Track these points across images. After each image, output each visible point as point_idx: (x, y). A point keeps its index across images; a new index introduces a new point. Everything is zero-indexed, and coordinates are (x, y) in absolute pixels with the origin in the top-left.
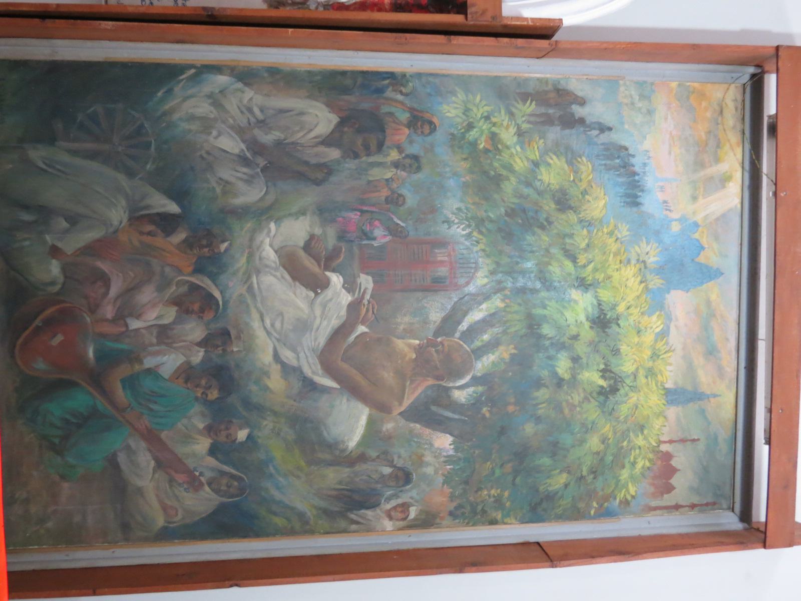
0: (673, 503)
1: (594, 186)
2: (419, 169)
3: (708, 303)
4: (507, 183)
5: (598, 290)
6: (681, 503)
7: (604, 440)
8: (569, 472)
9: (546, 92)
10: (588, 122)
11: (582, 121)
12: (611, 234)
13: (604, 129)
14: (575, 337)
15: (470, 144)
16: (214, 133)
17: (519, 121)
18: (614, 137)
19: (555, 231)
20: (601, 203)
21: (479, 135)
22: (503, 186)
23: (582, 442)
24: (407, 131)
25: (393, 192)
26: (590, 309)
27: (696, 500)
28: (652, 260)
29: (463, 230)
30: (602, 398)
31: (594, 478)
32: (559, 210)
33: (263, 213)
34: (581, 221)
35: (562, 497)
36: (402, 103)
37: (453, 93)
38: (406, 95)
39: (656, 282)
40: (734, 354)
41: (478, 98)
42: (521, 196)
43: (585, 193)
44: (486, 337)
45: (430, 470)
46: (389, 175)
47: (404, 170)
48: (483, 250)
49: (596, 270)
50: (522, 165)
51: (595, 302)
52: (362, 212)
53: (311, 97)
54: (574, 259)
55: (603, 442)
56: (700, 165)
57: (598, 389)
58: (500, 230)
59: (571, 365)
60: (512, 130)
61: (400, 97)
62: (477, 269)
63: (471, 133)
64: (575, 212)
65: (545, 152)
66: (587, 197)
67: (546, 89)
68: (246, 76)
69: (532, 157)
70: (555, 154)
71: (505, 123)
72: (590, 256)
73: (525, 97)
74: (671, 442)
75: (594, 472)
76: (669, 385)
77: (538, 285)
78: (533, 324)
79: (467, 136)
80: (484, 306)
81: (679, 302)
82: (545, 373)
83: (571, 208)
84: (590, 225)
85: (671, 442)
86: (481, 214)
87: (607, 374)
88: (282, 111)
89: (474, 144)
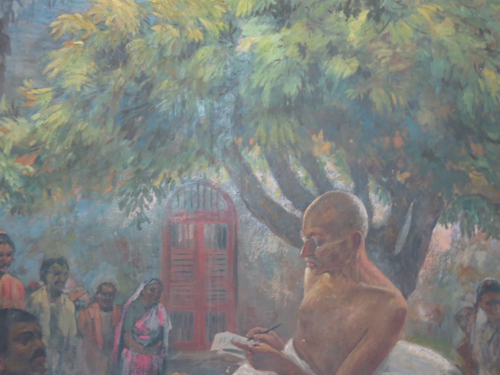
1: (91, 13)
2: (62, 261)
4: (85, 136)
5: (238, 14)
8: (482, 66)
14: (302, 49)
15: (27, 185)
19: (155, 69)
22: (89, 142)
23: (441, 46)
25: (95, 300)
26: (264, 27)
29: (151, 200)
30: (384, 17)
31: (489, 32)
32: (125, 63)
34: (142, 33)
42: (104, 117)
43: (101, 26)
44: (301, 173)
45: (481, 257)
46: (70, 306)
48: (180, 173)
49: (210, 17)
50: (60, 113)
51: (254, 19)
52: (123, 345)
54: (195, 46)
55: (442, 18)
57: (372, 22)
58: (151, 148)
59: (340, 56)
62: (207, 183)
63: (12, 183)
64: (128, 41)
66: (107, 23)
69: (49, 97)
70: (45, 65)
72: (191, 22)
75: (481, 33)
77: (229, 97)
78: (284, 107)
79: (15, 189)
80: (258, 175)
82: (351, 93)
84: (146, 21)
86: (125, 175)
87: (352, 7)
89: (28, 180)
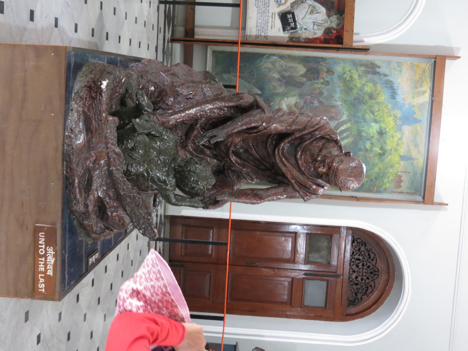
0: (401, 191)
2: (328, 85)
3: (416, 130)
4: (354, 90)
6: (404, 191)
7: (380, 169)
8: (368, 178)
9: (368, 64)
10: (380, 73)
11: (379, 73)
12: (386, 107)
13: (385, 75)
14: (372, 137)
15: (344, 78)
16: (272, 72)
17: (359, 72)
18: (388, 78)
19: (368, 105)
20: (383, 97)
21: (347, 76)
24: (326, 74)
25: (320, 91)
26: (377, 129)
27: (409, 191)
28: (399, 115)
30: (380, 156)
31: (376, 180)
33: (284, 95)
34: (376, 103)
35: (365, 185)
36: (325, 66)
37: (340, 64)
38: (326, 64)
39: (399, 122)
40: (424, 147)
41: (347, 65)
42: (358, 94)
43: (378, 94)
44: (345, 135)
46: (320, 86)
47: (324, 85)
49: (380, 117)
51: (379, 127)
52: (311, 96)
53: (299, 63)
54: (373, 114)
55: (379, 170)
56: (416, 87)
57: (379, 153)
59: (371, 145)
60: (357, 75)
61: (324, 64)
62: (343, 114)
64: (375, 100)
65: (367, 82)
67: (368, 63)
68: (282, 57)
71: (355, 73)
72: (379, 113)
73: (361, 65)
74: (401, 172)
75: (376, 178)
76: (402, 154)
77: (362, 121)
78: (359, 133)
80: (345, 126)
81: (406, 129)
82: (362, 147)
83: (373, 98)
84: (379, 104)
85: (401, 172)
86: (346, 99)
88: (291, 67)
89: (345, 78)
